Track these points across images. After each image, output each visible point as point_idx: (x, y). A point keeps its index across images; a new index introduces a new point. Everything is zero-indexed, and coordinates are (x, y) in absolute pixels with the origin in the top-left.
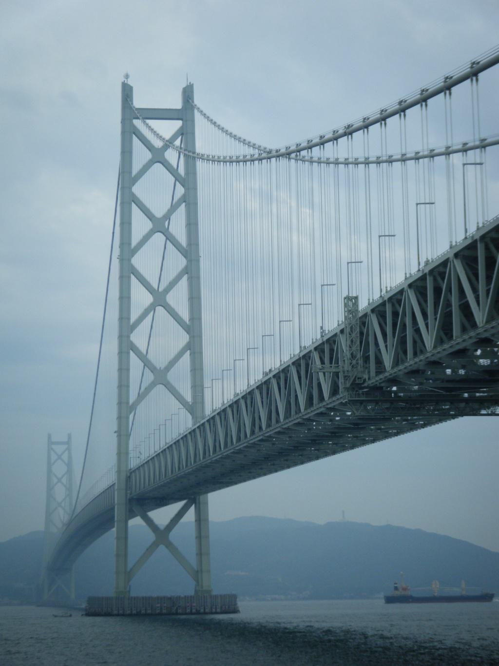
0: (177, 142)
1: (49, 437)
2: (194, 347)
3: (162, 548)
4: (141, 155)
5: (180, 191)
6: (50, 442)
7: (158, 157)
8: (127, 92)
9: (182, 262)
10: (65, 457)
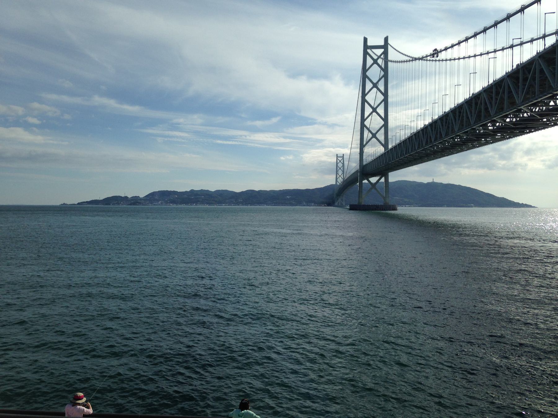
0: (382, 56)
1: (337, 155)
2: (386, 126)
4: (369, 61)
5: (382, 73)
7: (375, 62)
8: (365, 40)
9: (383, 97)
10: (342, 161)
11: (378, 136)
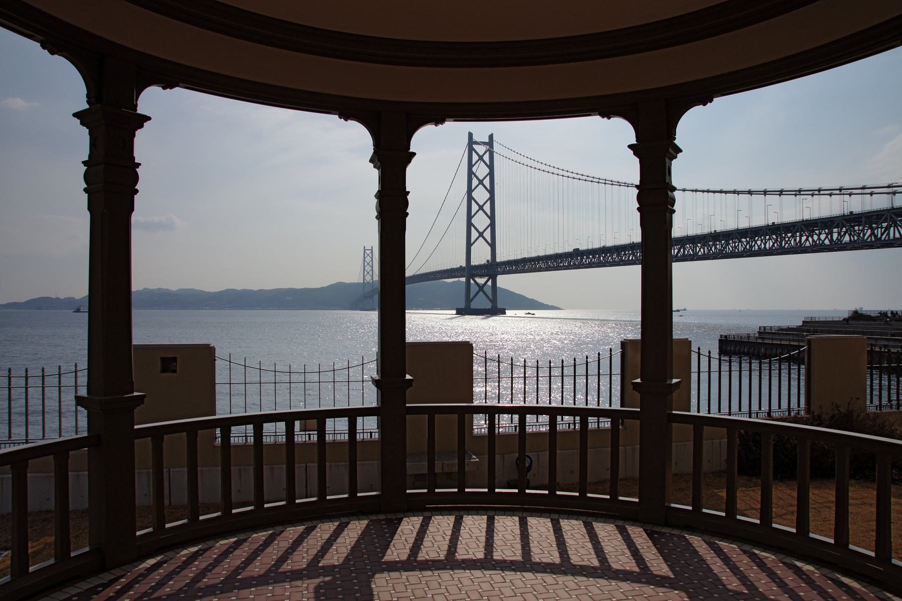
1: (364, 247)
3: (481, 293)
4: (475, 158)
7: (481, 158)
11: (485, 235)
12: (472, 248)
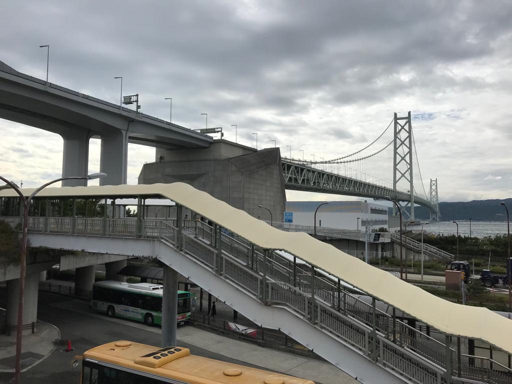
6: (431, 181)
8: (396, 114)
10: (435, 184)
12: (397, 184)
